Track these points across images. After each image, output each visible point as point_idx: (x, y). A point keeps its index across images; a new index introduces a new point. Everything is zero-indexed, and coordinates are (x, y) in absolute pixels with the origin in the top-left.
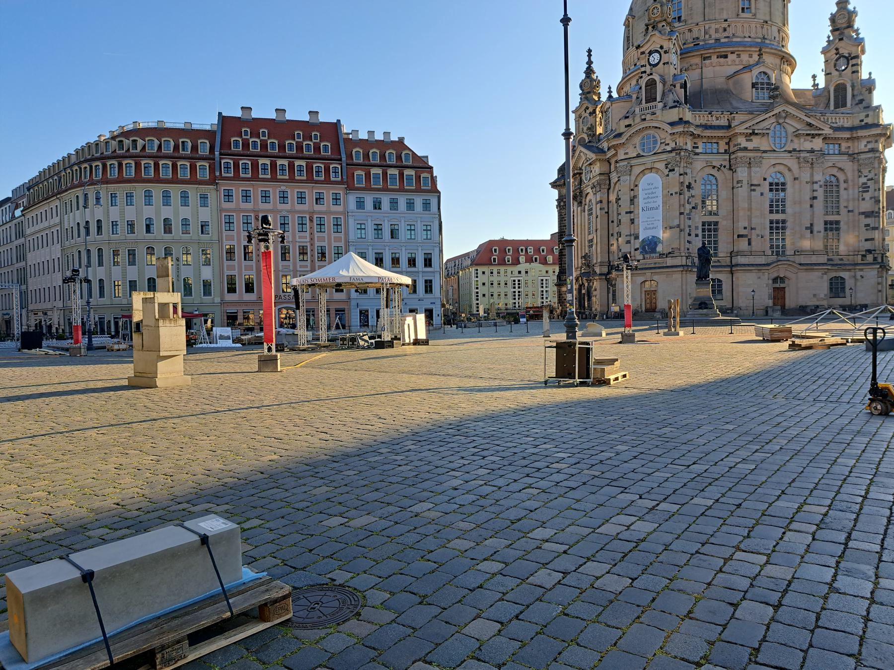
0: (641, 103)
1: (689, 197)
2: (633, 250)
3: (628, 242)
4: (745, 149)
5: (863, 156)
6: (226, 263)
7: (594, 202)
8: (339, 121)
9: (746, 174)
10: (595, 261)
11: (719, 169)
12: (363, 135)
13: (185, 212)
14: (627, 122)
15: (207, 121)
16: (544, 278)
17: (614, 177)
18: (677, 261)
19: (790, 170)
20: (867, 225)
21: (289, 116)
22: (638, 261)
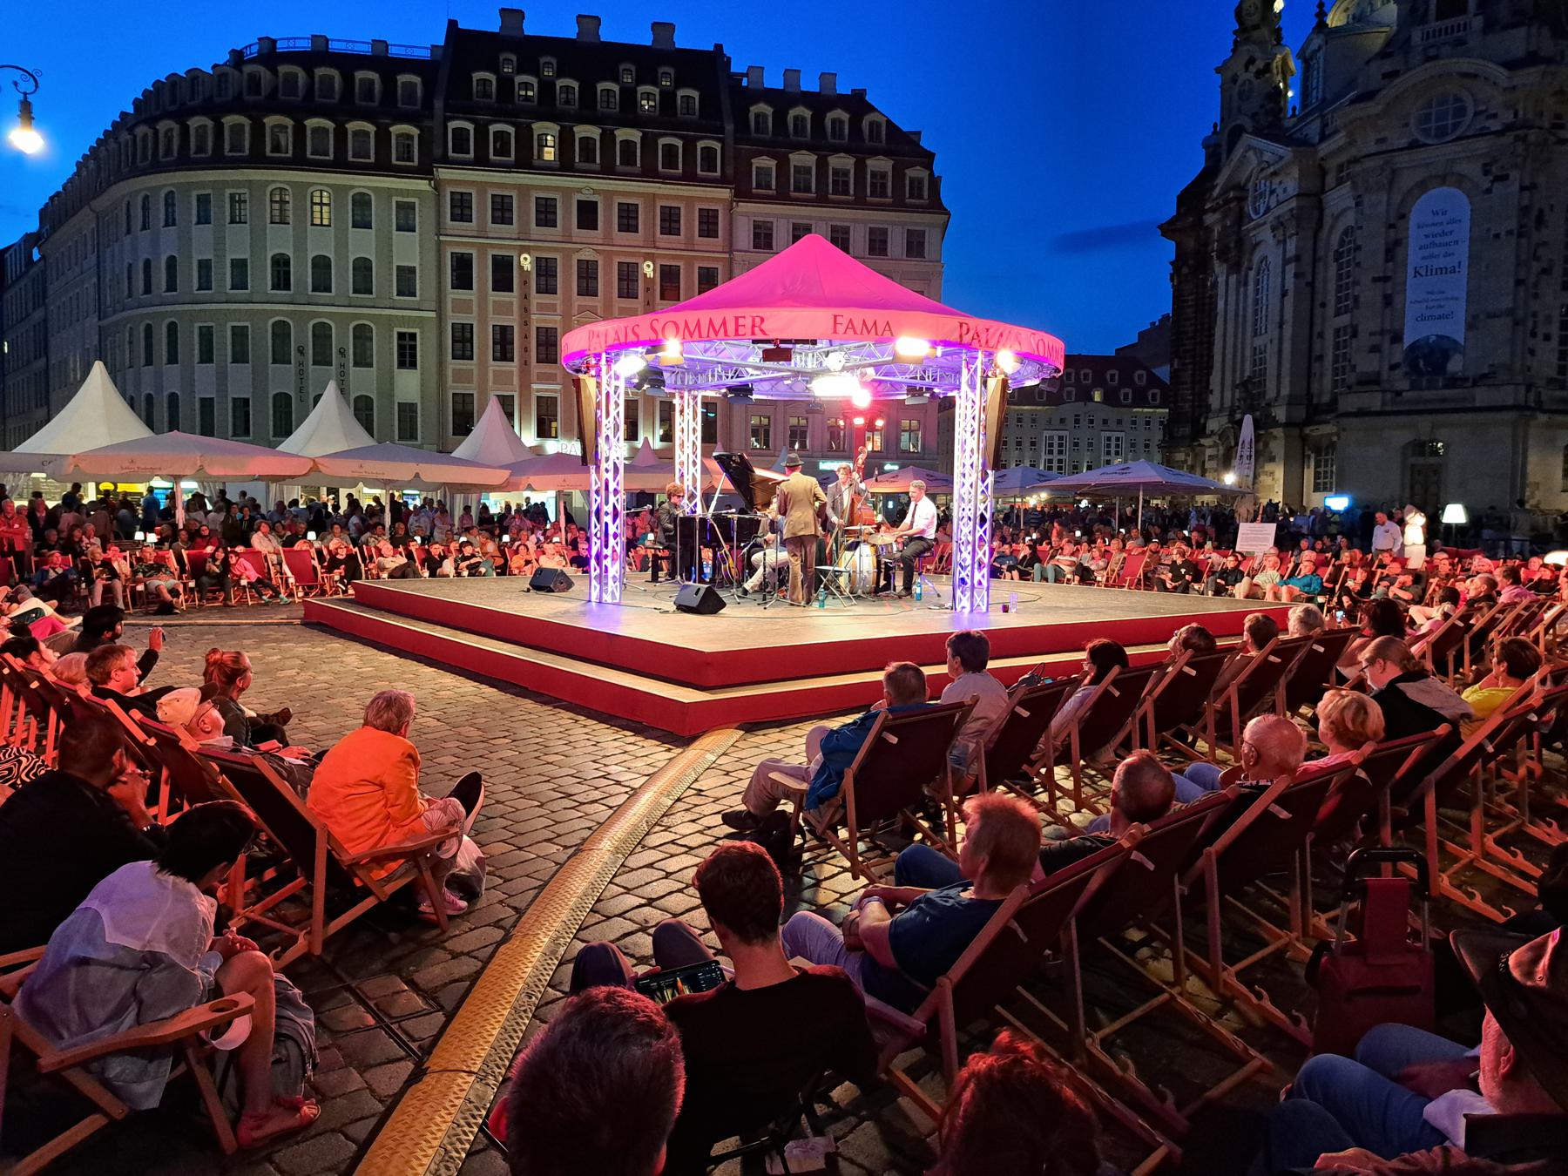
0: (1423, 20)
1: (1538, 245)
2: (1386, 367)
3: (1375, 349)
6: (452, 365)
7: (1275, 259)
8: (719, 47)
10: (1271, 393)
12: (774, 81)
13: (362, 244)
14: (1388, 66)
15: (419, 36)
16: (1114, 435)
17: (1339, 199)
18: (1507, 395)
21: (606, 35)
22: (1399, 393)
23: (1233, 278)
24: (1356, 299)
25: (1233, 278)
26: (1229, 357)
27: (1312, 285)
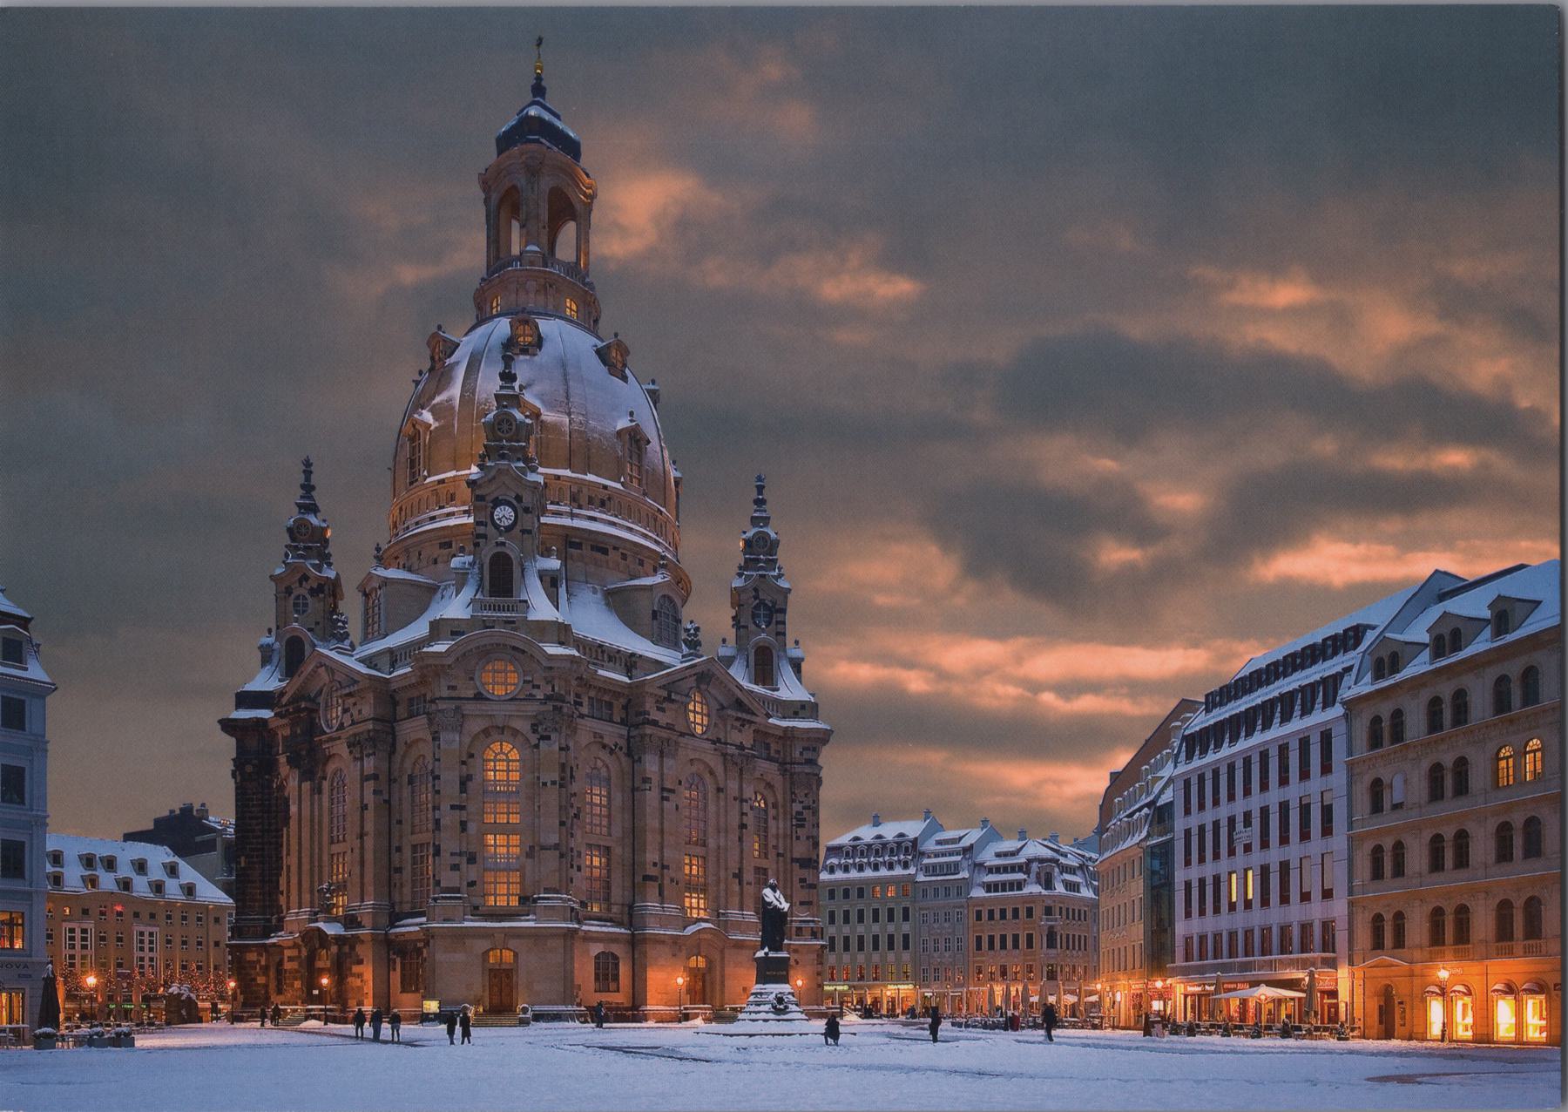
3: (455, 867)
4: (655, 723)
5: (798, 769)
9: (655, 768)
11: (612, 752)
19: (712, 773)
20: (803, 880)
23: (306, 785)
24: (437, 822)
25: (306, 785)
26: (306, 860)
27: (388, 802)
